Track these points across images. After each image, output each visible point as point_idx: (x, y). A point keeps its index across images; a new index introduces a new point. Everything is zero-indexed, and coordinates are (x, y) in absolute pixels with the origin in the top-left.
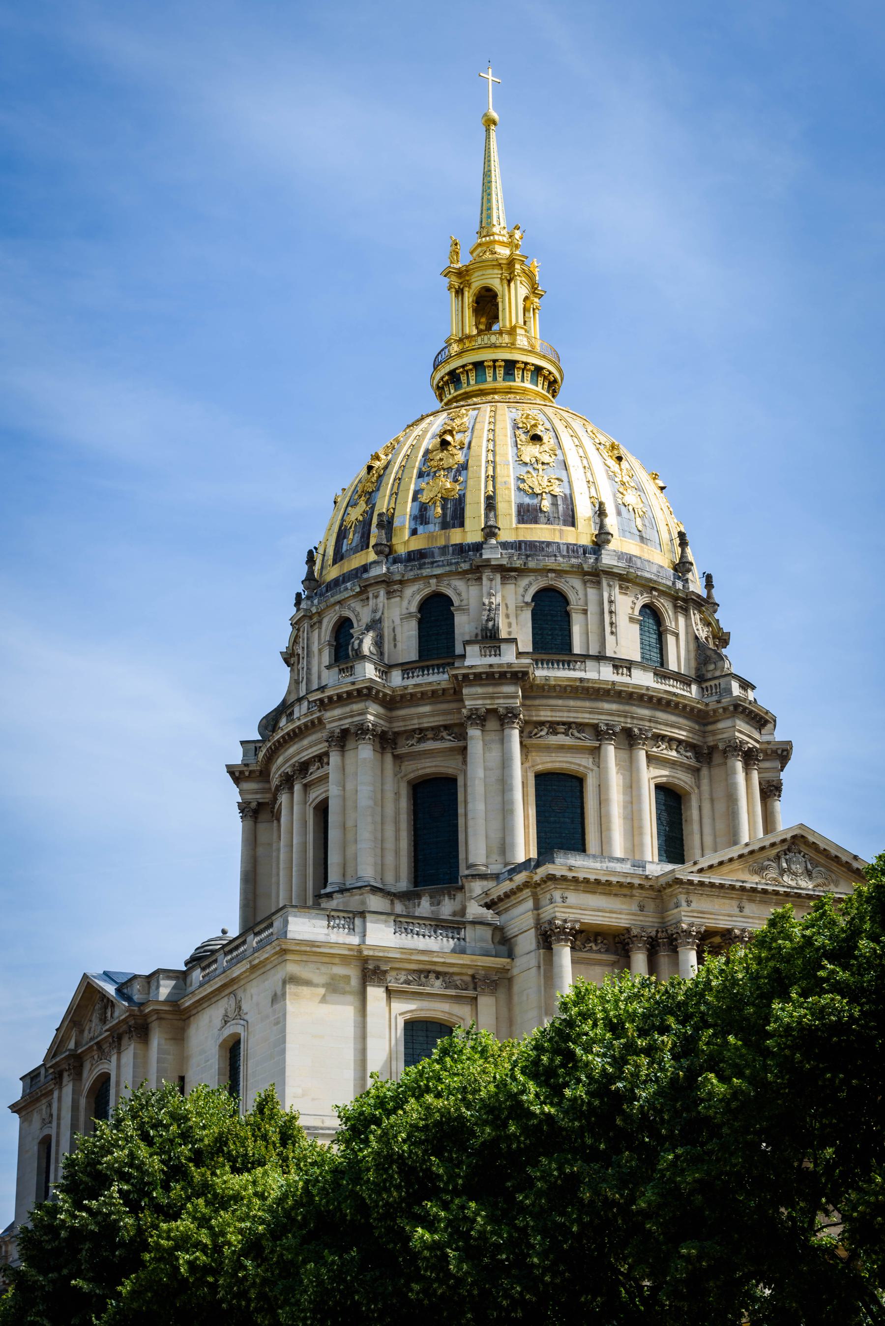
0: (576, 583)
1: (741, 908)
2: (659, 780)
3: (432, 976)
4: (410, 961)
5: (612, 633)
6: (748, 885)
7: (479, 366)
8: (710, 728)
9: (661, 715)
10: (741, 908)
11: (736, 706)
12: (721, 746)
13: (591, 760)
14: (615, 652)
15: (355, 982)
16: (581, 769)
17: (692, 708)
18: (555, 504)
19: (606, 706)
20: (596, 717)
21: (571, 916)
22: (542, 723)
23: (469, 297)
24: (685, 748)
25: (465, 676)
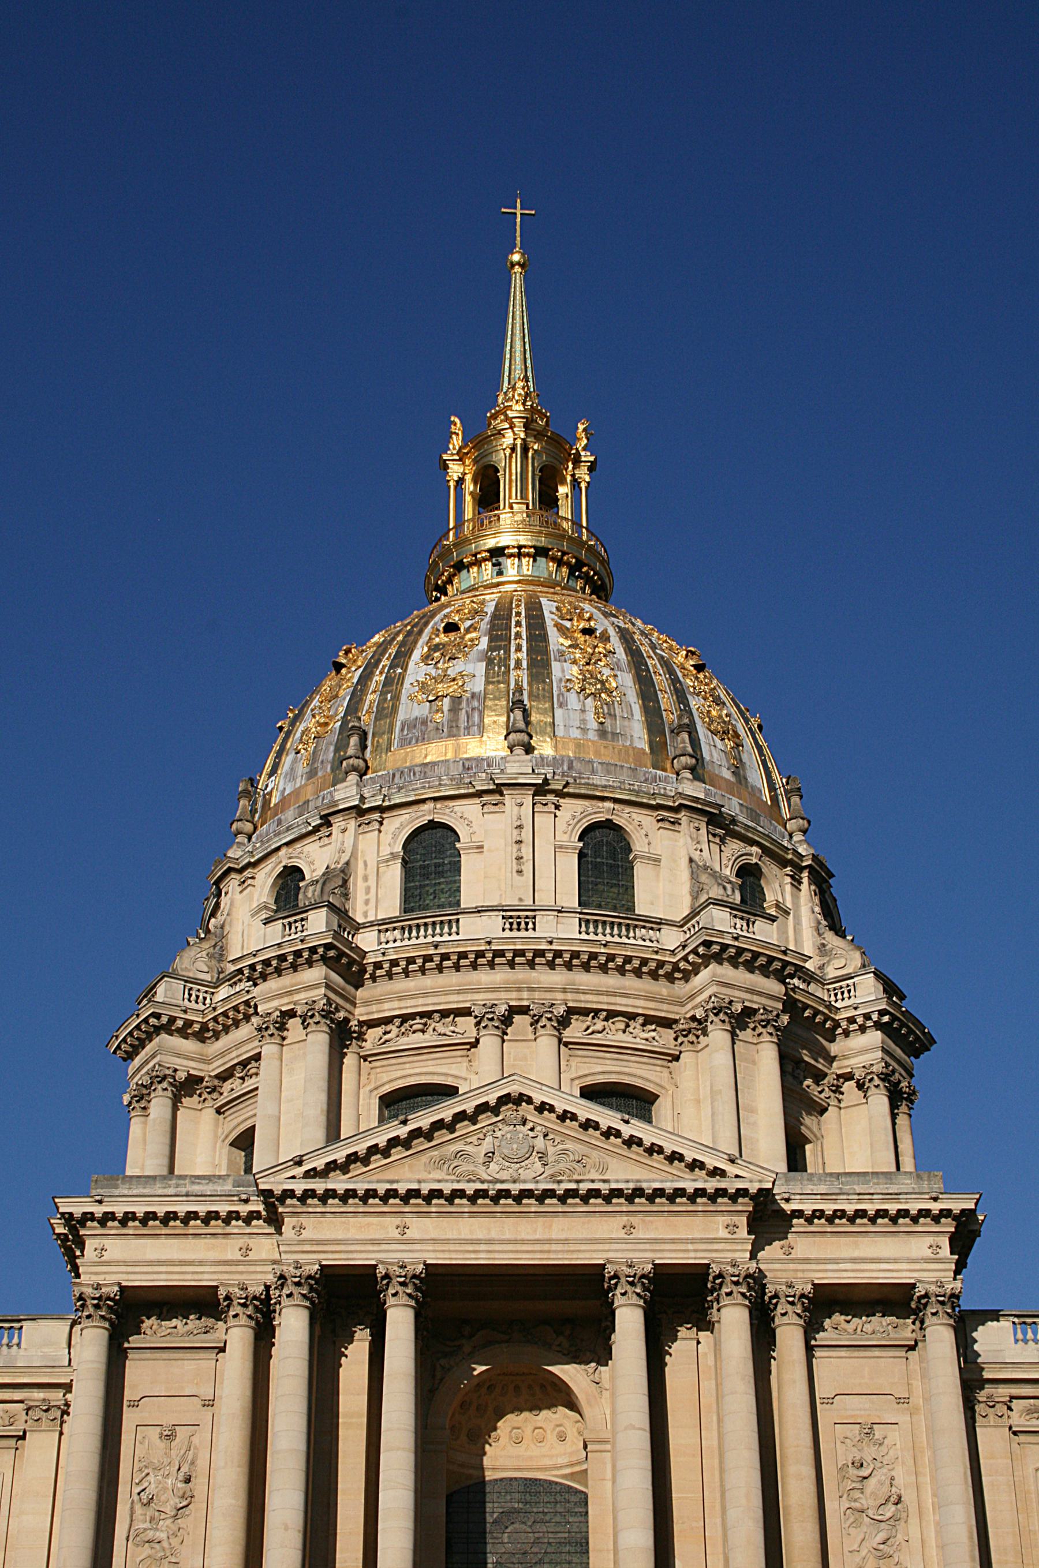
0: (471, 808)
2: (589, 1081)
5: (520, 872)
11: (707, 944)
12: (699, 1013)
13: (465, 1064)
14: (521, 900)
16: (450, 1081)
18: (455, 709)
19: (484, 977)
20: (469, 997)
21: (108, 1277)
22: (388, 1021)
23: (469, 486)
24: (643, 1025)
25: (252, 967)
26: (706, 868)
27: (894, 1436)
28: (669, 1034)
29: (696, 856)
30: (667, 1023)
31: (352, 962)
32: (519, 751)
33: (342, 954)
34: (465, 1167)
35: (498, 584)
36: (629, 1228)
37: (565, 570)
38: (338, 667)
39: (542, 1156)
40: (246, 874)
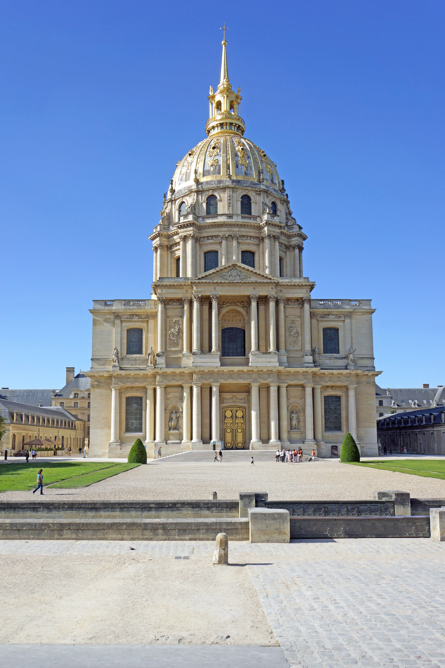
1: (215, 289)
3: (134, 316)
4: (128, 312)
6: (215, 281)
7: (213, 128)
8: (262, 231)
9: (243, 229)
10: (215, 289)
15: (112, 319)
16: (216, 249)
17: (254, 226)
18: (215, 168)
19: (223, 229)
22: (205, 237)
23: (214, 105)
25: (178, 226)
26: (266, 204)
27: (297, 322)
28: (258, 240)
29: (263, 201)
30: (258, 237)
31: (198, 225)
32: (228, 179)
33: (196, 224)
34: (226, 277)
35: (222, 132)
36: (254, 289)
37: (236, 128)
38: (190, 155)
39: (239, 276)
40: (174, 202)
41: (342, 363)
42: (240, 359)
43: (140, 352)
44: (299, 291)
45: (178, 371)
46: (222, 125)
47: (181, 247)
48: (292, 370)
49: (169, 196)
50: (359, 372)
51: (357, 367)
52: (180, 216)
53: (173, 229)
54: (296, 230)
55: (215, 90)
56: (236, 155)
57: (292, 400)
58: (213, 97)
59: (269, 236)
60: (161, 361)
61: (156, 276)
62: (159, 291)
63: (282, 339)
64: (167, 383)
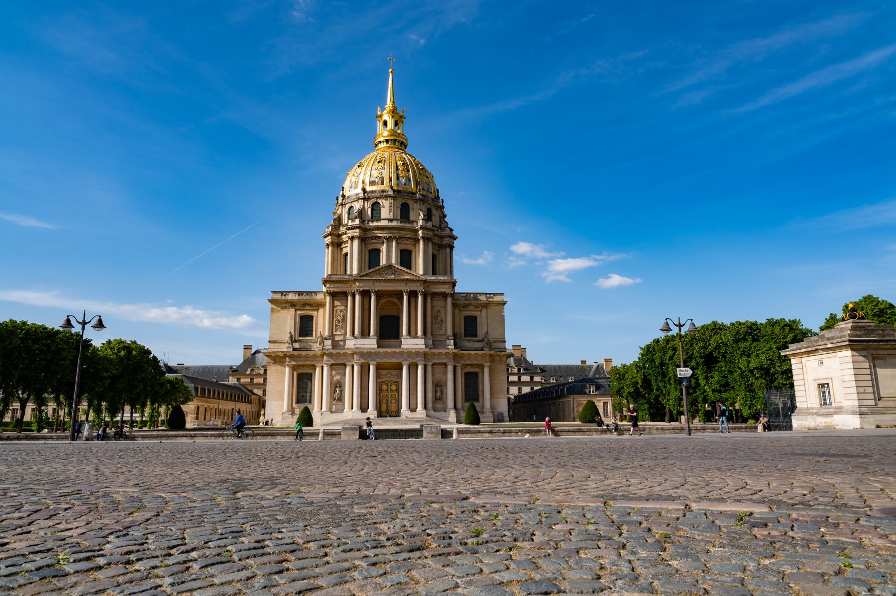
7: (380, 142)
23: (381, 123)
41: (479, 345)
42: (394, 342)
43: (311, 335)
44: (443, 286)
45: (342, 352)
46: (387, 141)
47: (349, 244)
48: (436, 351)
49: (340, 201)
50: (492, 352)
51: (491, 348)
52: (349, 219)
53: (342, 229)
54: (447, 231)
55: (383, 110)
56: (397, 169)
57: (437, 376)
58: (381, 116)
59: (423, 237)
60: (328, 343)
61: (327, 271)
62: (328, 285)
63: (429, 326)
64: (332, 362)
